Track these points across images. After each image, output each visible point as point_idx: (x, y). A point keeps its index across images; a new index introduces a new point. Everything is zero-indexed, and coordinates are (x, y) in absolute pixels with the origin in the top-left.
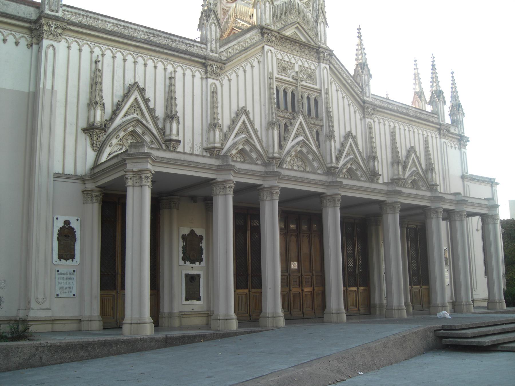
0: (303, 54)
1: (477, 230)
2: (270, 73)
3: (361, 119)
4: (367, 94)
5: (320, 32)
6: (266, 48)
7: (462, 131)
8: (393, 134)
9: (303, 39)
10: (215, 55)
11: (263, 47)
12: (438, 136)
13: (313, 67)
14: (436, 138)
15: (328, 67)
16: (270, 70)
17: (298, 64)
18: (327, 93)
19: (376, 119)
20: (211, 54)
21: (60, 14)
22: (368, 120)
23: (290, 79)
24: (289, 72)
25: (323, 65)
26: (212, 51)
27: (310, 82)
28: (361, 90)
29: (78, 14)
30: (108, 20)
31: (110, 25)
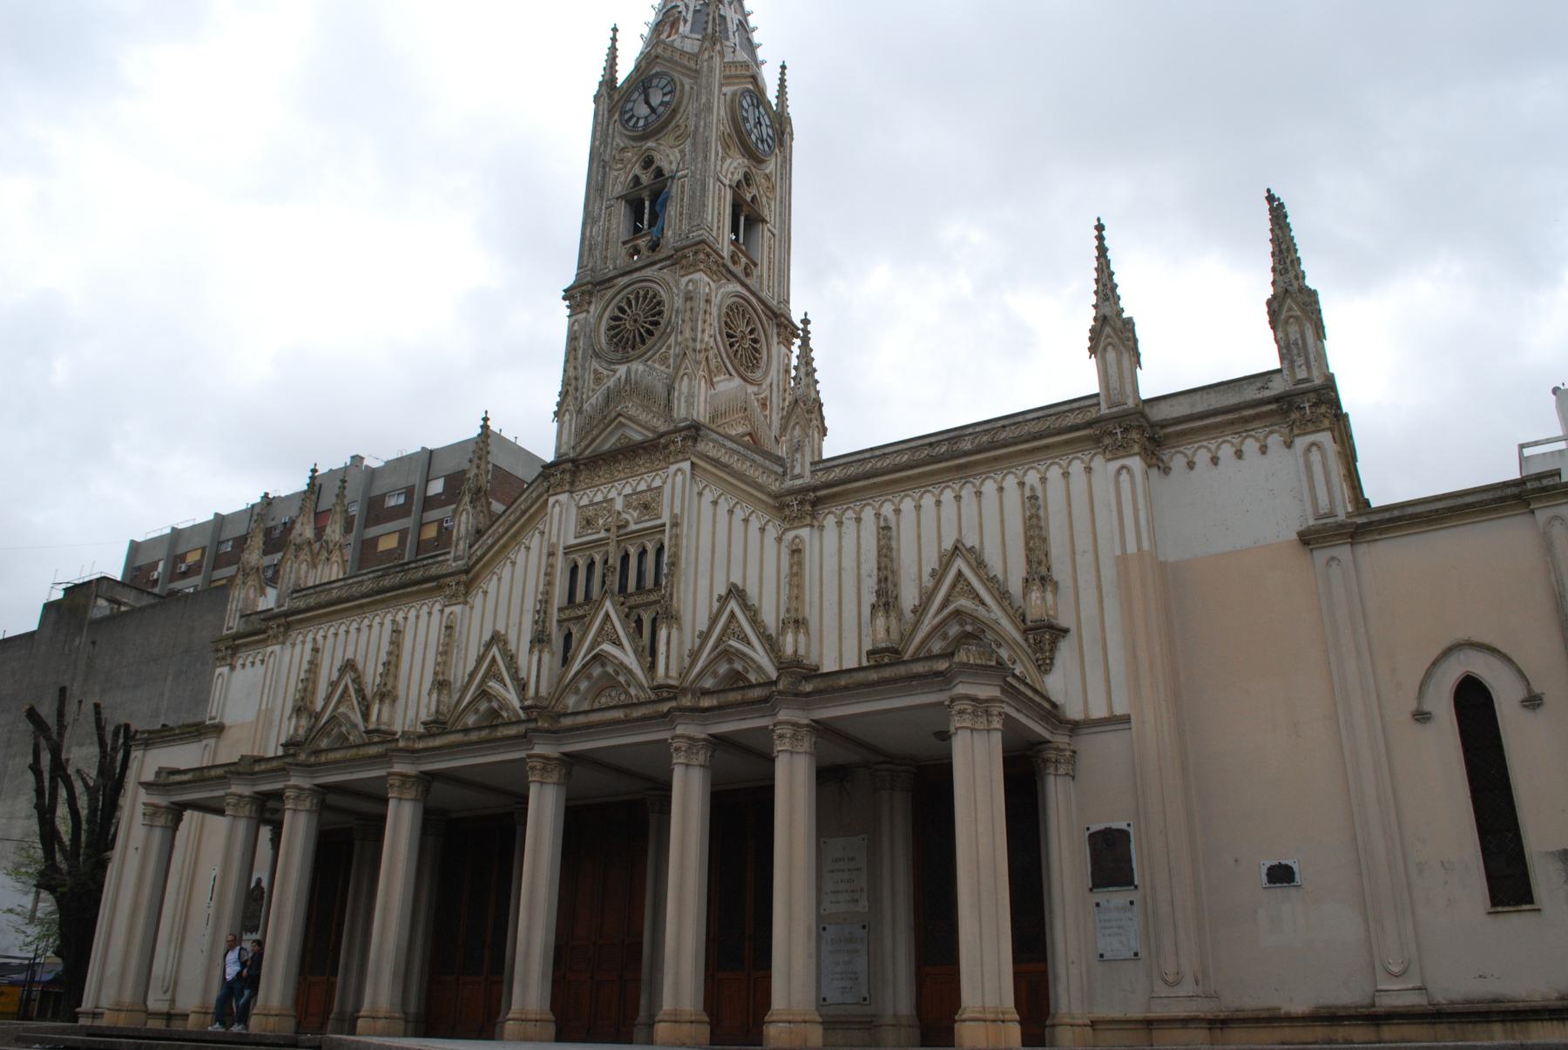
0: (657, 463)
1: (1421, 716)
2: (553, 545)
3: (779, 540)
4: (797, 471)
5: (679, 400)
6: (552, 500)
7: (1302, 374)
8: (885, 531)
9: (638, 438)
10: (460, 563)
11: (547, 500)
12: (1098, 462)
13: (657, 483)
14: (1088, 470)
15: (686, 466)
16: (554, 540)
17: (622, 496)
18: (675, 525)
19: (830, 521)
20: (454, 565)
21: (285, 608)
22: (790, 535)
23: (603, 534)
24: (601, 522)
25: (673, 468)
26: (455, 559)
27: (647, 517)
28: (780, 470)
29: (304, 596)
30: (335, 585)
31: (335, 591)
